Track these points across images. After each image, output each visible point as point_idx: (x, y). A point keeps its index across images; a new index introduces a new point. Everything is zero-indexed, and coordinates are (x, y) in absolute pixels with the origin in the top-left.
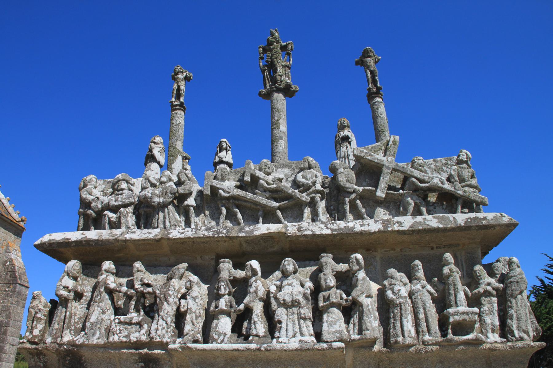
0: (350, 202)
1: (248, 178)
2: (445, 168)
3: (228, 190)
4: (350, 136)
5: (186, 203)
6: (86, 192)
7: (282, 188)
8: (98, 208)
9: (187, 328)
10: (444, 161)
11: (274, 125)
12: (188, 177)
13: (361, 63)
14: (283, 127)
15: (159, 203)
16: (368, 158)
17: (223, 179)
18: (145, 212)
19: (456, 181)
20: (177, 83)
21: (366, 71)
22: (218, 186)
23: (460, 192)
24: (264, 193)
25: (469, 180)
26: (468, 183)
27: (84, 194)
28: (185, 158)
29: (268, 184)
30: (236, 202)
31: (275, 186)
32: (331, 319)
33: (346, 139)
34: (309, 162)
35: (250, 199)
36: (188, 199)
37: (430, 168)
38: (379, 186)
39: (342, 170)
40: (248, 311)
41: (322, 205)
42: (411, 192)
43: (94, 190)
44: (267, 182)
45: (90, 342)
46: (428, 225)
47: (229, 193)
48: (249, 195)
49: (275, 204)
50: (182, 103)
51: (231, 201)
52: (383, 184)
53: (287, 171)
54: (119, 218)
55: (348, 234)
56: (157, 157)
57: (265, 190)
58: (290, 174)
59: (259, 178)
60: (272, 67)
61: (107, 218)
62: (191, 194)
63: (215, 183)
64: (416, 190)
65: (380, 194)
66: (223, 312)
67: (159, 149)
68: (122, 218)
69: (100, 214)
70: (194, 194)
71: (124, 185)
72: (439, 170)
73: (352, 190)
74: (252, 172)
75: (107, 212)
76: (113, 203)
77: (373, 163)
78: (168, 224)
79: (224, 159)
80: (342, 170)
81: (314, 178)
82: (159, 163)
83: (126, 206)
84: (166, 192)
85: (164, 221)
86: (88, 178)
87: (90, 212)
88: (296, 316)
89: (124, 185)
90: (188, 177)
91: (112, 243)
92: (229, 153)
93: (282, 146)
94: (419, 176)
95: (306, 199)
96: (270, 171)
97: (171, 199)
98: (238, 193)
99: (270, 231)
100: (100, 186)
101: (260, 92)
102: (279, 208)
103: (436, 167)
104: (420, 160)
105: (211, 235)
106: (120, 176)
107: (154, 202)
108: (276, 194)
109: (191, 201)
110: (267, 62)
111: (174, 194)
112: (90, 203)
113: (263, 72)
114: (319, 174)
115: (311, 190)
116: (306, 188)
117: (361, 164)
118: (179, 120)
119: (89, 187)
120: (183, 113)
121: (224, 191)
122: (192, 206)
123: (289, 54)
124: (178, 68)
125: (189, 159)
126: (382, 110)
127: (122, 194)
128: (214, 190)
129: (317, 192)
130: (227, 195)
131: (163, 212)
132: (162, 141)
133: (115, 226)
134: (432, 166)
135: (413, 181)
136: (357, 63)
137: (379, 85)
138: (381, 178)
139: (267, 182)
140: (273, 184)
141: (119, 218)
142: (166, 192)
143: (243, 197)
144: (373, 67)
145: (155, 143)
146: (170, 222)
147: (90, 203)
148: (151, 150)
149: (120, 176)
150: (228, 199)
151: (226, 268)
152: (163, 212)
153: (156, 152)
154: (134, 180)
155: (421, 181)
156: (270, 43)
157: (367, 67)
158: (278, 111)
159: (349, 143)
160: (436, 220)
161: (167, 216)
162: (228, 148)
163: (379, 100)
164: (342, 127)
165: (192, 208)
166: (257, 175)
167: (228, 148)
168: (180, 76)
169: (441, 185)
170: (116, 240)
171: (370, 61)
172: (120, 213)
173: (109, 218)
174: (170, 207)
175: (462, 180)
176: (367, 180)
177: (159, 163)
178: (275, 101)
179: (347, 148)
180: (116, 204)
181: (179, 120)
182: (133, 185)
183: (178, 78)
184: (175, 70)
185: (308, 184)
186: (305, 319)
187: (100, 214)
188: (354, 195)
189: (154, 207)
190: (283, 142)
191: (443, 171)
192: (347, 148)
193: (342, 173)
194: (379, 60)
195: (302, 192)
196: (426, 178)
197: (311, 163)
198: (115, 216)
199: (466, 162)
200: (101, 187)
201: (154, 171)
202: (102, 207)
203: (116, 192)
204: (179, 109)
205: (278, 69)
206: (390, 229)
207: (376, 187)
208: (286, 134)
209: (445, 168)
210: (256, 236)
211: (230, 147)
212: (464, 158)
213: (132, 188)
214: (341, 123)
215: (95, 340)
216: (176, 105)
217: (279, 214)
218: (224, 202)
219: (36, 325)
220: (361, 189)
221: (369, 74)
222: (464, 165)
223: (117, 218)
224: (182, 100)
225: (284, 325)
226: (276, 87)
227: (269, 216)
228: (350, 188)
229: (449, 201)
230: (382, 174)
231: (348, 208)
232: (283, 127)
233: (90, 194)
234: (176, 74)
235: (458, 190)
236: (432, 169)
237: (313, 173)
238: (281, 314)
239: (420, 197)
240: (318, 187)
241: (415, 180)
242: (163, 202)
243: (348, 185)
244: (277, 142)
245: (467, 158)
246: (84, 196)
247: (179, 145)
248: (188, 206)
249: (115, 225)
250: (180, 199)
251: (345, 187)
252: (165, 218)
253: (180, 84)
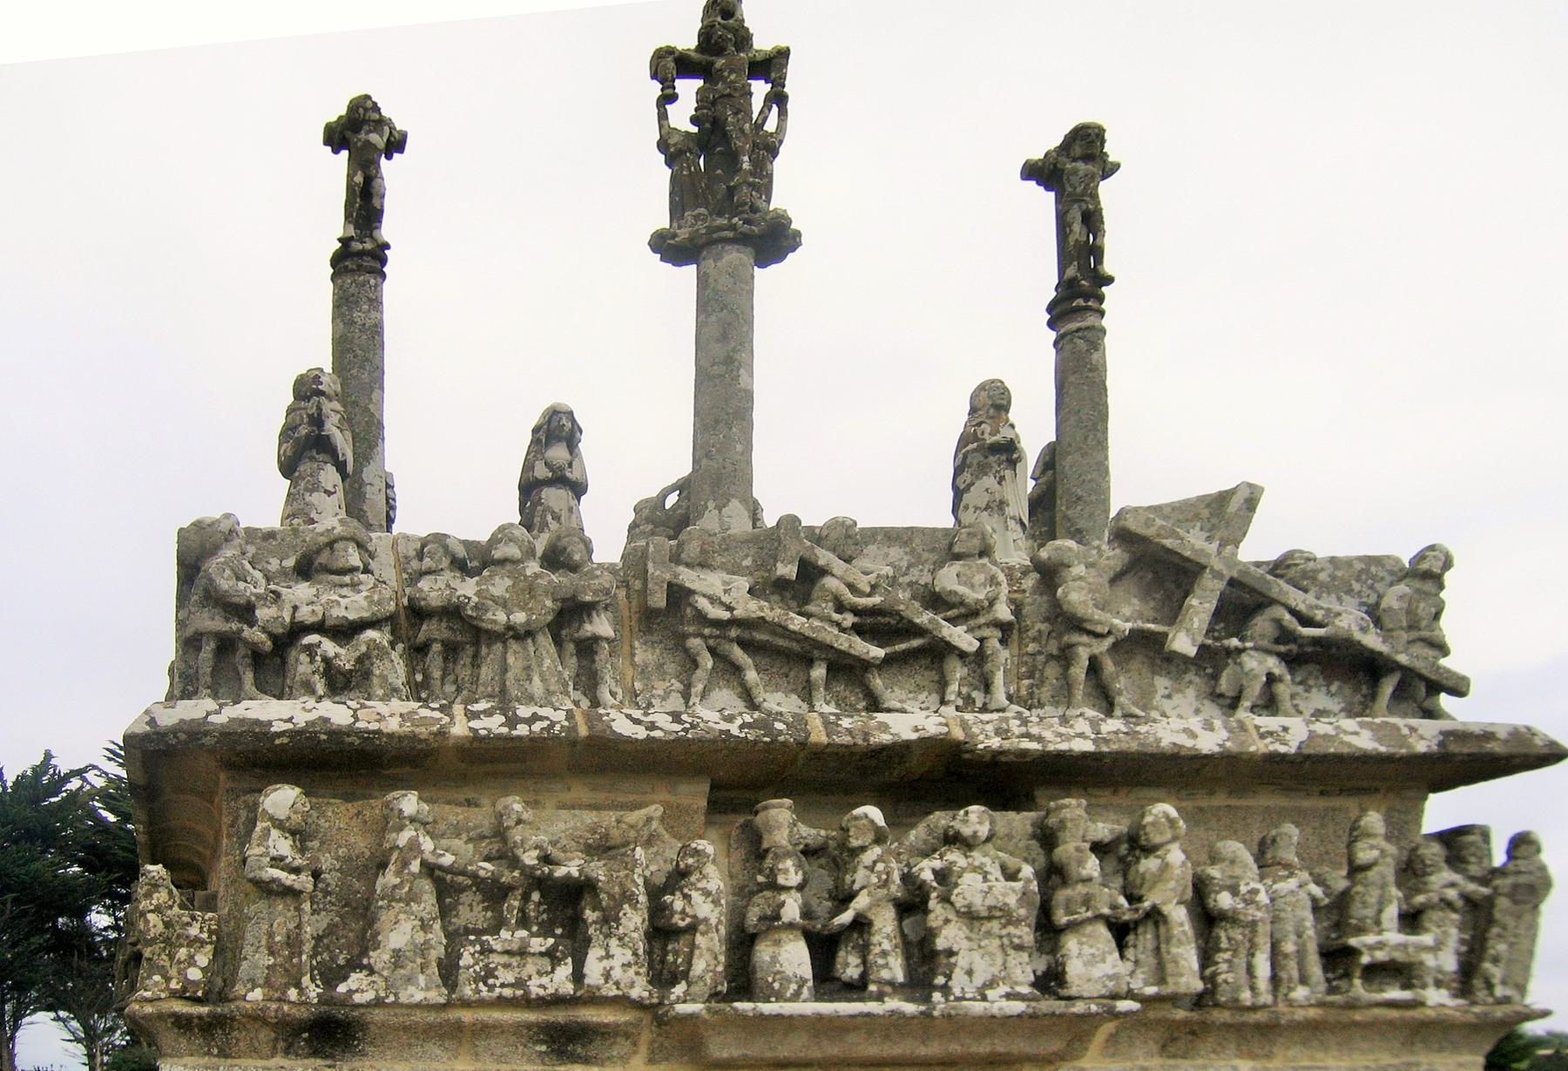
9: (699, 966)
24: (836, 617)
32: (1093, 951)
40: (861, 925)
45: (403, 999)
49: (877, 652)
57: (840, 607)
58: (904, 564)
66: (791, 926)
88: (997, 942)
94: (1302, 607)
108: (875, 624)
115: (982, 620)
116: (967, 614)
135: (1278, 622)
151: (782, 820)
155: (1306, 621)
186: (1019, 948)
195: (953, 621)
196: (1319, 615)
215: (414, 994)
218: (707, 631)
219: (192, 957)
225: (962, 961)
228: (1100, 623)
238: (950, 935)
240: (1003, 612)
241: (1287, 616)
248: (596, 639)
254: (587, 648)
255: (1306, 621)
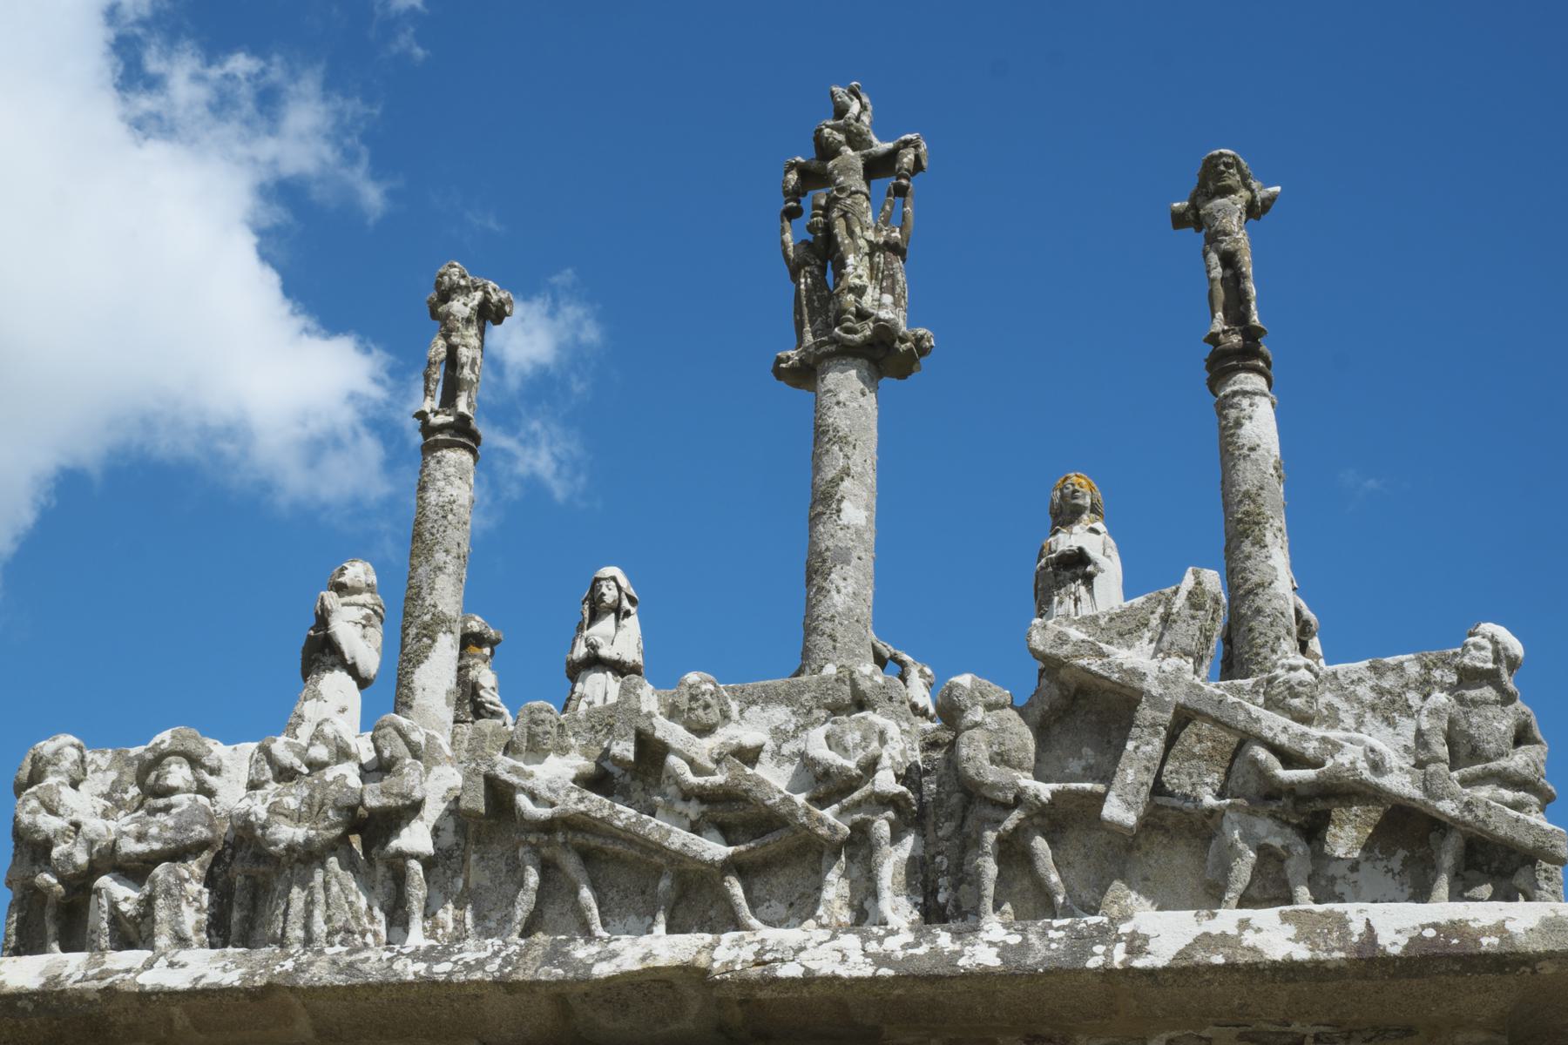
0: (999, 840)
1: (625, 749)
2: (1413, 698)
3: (547, 794)
4: (1094, 552)
5: (395, 844)
6: (34, 803)
7: (746, 785)
8: (75, 866)
10: (1413, 669)
11: (824, 500)
12: (408, 743)
13: (1192, 219)
14: (856, 512)
15: (291, 848)
16: (1083, 662)
17: (536, 749)
18: (245, 881)
19: (1437, 760)
20: (446, 337)
21: (1205, 255)
22: (513, 779)
23: (1448, 807)
24: (680, 806)
25: (1500, 755)
26: (1493, 765)
27: (30, 812)
28: (469, 641)
29: (697, 770)
30: (579, 839)
31: (719, 778)
33: (1077, 565)
34: (854, 684)
35: (626, 830)
36: (405, 832)
37: (1351, 698)
38: (1117, 781)
39: (977, 714)
41: (893, 860)
42: (1246, 804)
43: (67, 795)
44: (691, 762)
46: (1253, 949)
47: (553, 805)
48: (625, 814)
49: (714, 849)
50: (463, 419)
51: (560, 838)
52: (1133, 773)
53: (781, 714)
54: (148, 903)
55: (932, 979)
56: (345, 647)
57: (688, 794)
58: (791, 727)
59: (663, 749)
60: (823, 252)
61: (104, 902)
62: (416, 808)
63: (503, 765)
64: (1270, 794)
65: (1119, 810)
67: (357, 614)
68: (160, 902)
69: (81, 885)
70: (433, 811)
71: (178, 774)
72: (1389, 707)
73: (1011, 797)
74: (643, 724)
75: (105, 881)
76: (130, 846)
77: (1107, 684)
78: (320, 927)
79: (604, 652)
80: (977, 714)
81: (875, 744)
82: (352, 670)
83: (178, 854)
84: (322, 804)
85: (309, 915)
86: (47, 747)
87: (48, 878)
89: (178, 774)
90: (408, 743)
91: (92, 1003)
92: (632, 624)
93: (849, 591)
94: (1283, 739)
95: (833, 828)
96: (713, 716)
97: (338, 831)
98: (581, 807)
99: (651, 963)
100: (100, 775)
101: (779, 360)
102: (732, 866)
103: (1380, 692)
104: (1293, 668)
105: (442, 978)
106: (165, 738)
107: (275, 844)
108: (727, 810)
109: (416, 838)
110: (811, 228)
111: (352, 809)
112: (48, 844)
113: (795, 276)
114: (893, 729)
115: (856, 795)
117: (1062, 685)
118: (449, 490)
119: (51, 780)
120: (466, 457)
121: (534, 797)
122: (416, 856)
123: (900, 191)
124: (455, 273)
125: (493, 643)
126: (1261, 425)
127: (167, 809)
128: (499, 794)
129: (884, 801)
130: (544, 813)
131: (305, 884)
132: (373, 579)
133: (134, 936)
134: (1364, 691)
135: (1255, 762)
136: (1179, 220)
137: (1255, 319)
138: (1130, 745)
139: (691, 762)
140: (712, 773)
141: (148, 903)
142: (322, 804)
143: (603, 819)
144: (1239, 236)
145: (341, 589)
146: (328, 920)
147: (48, 844)
148: (323, 619)
149: (165, 738)
150: (548, 826)
152: (305, 884)
153: (347, 627)
154: (218, 751)
155: (1290, 759)
156: (826, 151)
157: (1213, 238)
158: (843, 441)
159: (1088, 580)
160: (1291, 930)
161: (320, 896)
162: (626, 604)
163: (1255, 382)
164: (1066, 514)
165: (415, 866)
166: (658, 734)
167: (626, 604)
168: (460, 307)
169: (1367, 775)
170: (110, 992)
171: (1229, 211)
172: (153, 882)
173: (114, 905)
174: (333, 862)
175: (1463, 749)
176: (1087, 751)
177: (352, 670)
178: (827, 400)
179: (1077, 600)
180: (141, 848)
181: (449, 490)
182: (214, 771)
183: (449, 314)
184: (438, 284)
185: (842, 769)
187: (81, 885)
188: (1016, 816)
189: (275, 860)
190: (849, 570)
191: (1408, 710)
192: (1077, 600)
193: (976, 725)
194: (1272, 199)
196: (1311, 748)
197: (865, 685)
198: (135, 895)
199: (1491, 677)
200: (99, 781)
201: (334, 703)
202: (91, 862)
203: (151, 802)
204: (449, 445)
205: (851, 260)
206: (1092, 963)
207: (1107, 778)
208: (870, 537)
209: (1413, 698)
210: (598, 981)
211: (632, 600)
212: (1482, 659)
213: (212, 781)
214: (1063, 497)
216: (441, 428)
217: (736, 889)
218: (532, 839)
220: (1045, 790)
221: (1217, 272)
222: (1488, 692)
223: (140, 902)
224: (462, 406)
226: (835, 341)
227: (694, 899)
228: (1002, 788)
229: (1413, 844)
230: (1135, 731)
231: (990, 868)
232: (856, 512)
233: (53, 812)
234: (445, 296)
235: (1441, 798)
236: (1361, 702)
237: (871, 725)
239: (1287, 823)
240: (886, 782)
241: (1262, 754)
242: (308, 841)
243: (992, 774)
244: (826, 576)
245: (1497, 660)
246: (26, 819)
247: (446, 595)
248: (403, 856)
249: (132, 932)
250: (369, 830)
251: (983, 784)
252: (310, 904)
253: (455, 339)
254: (397, 866)
255: (1290, 759)
